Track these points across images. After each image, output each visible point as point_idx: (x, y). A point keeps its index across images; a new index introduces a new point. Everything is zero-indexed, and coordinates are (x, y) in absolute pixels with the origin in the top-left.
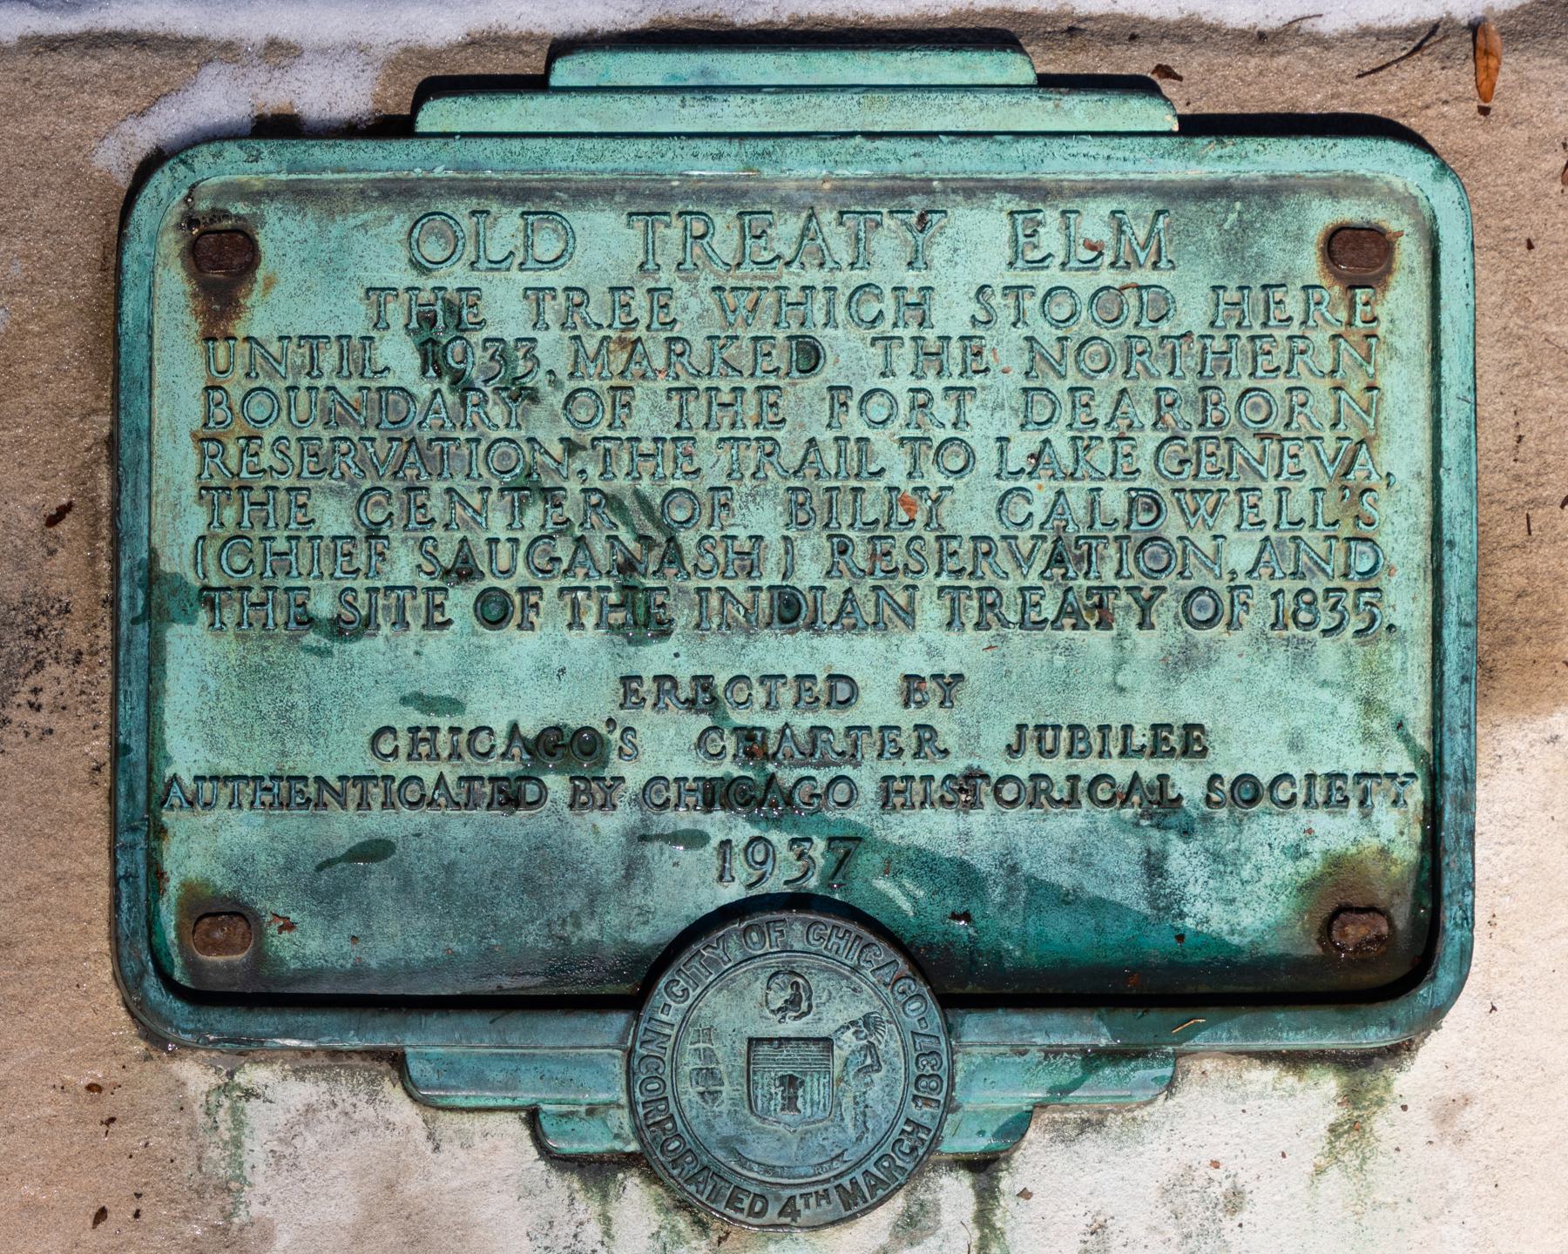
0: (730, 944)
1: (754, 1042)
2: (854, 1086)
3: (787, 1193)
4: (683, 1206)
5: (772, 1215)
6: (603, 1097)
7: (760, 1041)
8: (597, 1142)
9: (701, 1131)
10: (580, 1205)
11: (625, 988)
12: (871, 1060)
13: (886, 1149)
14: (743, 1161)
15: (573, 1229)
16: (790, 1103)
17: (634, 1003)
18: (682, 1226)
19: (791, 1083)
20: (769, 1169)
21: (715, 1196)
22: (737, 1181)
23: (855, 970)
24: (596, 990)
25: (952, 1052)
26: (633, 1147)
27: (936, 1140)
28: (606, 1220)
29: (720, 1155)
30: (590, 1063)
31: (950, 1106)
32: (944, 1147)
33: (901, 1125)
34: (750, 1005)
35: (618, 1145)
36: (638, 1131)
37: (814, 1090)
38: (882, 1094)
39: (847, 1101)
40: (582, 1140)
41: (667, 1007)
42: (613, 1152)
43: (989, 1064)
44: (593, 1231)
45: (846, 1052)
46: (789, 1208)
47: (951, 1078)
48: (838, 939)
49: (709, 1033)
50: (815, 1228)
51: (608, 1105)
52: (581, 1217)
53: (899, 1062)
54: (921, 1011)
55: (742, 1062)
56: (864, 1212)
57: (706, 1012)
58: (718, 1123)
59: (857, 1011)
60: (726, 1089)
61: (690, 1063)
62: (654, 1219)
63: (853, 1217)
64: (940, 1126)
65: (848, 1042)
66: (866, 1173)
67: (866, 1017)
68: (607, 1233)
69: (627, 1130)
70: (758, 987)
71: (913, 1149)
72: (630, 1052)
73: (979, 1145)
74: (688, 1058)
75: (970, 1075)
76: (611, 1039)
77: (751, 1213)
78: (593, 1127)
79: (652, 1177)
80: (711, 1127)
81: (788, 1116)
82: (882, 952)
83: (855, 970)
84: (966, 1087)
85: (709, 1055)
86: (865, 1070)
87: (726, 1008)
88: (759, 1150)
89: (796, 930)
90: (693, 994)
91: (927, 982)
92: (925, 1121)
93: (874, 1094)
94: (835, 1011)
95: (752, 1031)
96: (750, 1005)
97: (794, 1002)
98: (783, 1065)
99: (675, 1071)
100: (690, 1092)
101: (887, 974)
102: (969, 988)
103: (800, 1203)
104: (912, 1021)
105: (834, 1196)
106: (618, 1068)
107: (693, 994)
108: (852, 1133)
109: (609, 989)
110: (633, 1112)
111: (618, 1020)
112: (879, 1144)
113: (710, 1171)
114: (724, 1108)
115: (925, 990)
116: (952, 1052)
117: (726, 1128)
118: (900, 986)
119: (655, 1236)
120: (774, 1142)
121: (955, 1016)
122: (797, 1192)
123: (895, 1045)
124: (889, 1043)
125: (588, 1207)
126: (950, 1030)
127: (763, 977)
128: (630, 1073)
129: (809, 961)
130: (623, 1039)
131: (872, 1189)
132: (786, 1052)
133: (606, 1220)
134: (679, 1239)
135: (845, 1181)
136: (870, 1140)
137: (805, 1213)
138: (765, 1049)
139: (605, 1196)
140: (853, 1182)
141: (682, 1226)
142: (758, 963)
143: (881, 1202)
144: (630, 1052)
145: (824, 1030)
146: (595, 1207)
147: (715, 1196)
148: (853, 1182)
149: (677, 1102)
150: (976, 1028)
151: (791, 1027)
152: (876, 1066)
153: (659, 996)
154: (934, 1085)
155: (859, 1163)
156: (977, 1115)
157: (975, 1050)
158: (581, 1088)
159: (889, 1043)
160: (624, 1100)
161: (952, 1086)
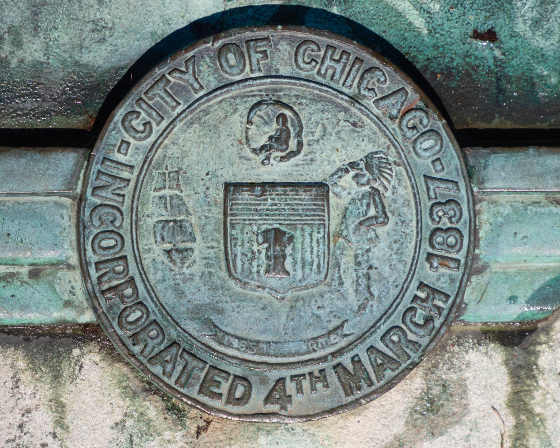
0: (203, 66)
1: (231, 188)
2: (356, 242)
3: (274, 375)
4: (151, 388)
5: (256, 402)
6: (50, 255)
7: (239, 186)
8: (43, 312)
9: (168, 298)
10: (26, 389)
11: (77, 121)
12: (375, 207)
13: (395, 319)
14: (219, 334)
15: (18, 418)
16: (277, 263)
17: (83, 139)
18: (152, 413)
19: (277, 238)
20: (254, 345)
21: (186, 378)
22: (212, 360)
23: (354, 99)
24: (40, 123)
25: (474, 201)
26: (88, 317)
27: (458, 307)
28: (59, 406)
29: (192, 327)
30: (32, 214)
31: (473, 267)
32: (468, 316)
33: (413, 290)
34: (226, 142)
35: (69, 315)
36: (91, 296)
37: (306, 245)
38: (390, 251)
39: (347, 261)
40: (25, 308)
41: (125, 143)
42: (65, 323)
43: (520, 214)
44: (42, 421)
45: (345, 201)
46: (277, 393)
47: (474, 232)
48: (335, 62)
49: (176, 177)
50: (308, 417)
51: (56, 265)
52: (28, 402)
53: (410, 213)
54: (435, 150)
55: (217, 213)
56: (369, 397)
57: (174, 151)
58: (189, 288)
59: (358, 150)
60: (198, 246)
61: (153, 213)
62: (115, 405)
63: (356, 403)
64: (460, 291)
65: (347, 189)
66: (371, 348)
67: (369, 157)
68: (60, 422)
69: (80, 296)
70: (237, 120)
71: (428, 320)
72: (81, 200)
73: (510, 314)
74: (151, 208)
75: (497, 229)
76: (57, 185)
77: (231, 399)
78: (38, 291)
79: (112, 354)
80: (180, 294)
81: (273, 280)
82: (388, 78)
83: (354, 99)
84: (492, 243)
85: (176, 204)
86: (366, 222)
87: (195, 148)
88: (240, 320)
89: (282, 49)
90: (157, 129)
91: (444, 113)
92: (443, 285)
93: (379, 252)
94: (331, 149)
95: (229, 176)
96: (226, 142)
97: (279, 140)
98: (272, 217)
99: (136, 224)
100: (153, 251)
101: (394, 105)
102: (497, 123)
103: (291, 387)
104: (424, 163)
105: (332, 377)
106: (67, 220)
107: (157, 129)
108: (353, 300)
109: (57, 122)
110: (85, 275)
111: (66, 160)
112: (386, 314)
113: (181, 348)
114: (197, 269)
115: (440, 124)
116: (474, 201)
117: (199, 295)
118: (410, 119)
119: (119, 425)
120: (258, 312)
121: (478, 156)
122: (286, 373)
123: (405, 192)
124: (398, 190)
125: (35, 390)
126: (470, 174)
127: (243, 108)
128: (81, 226)
129: (298, 88)
130: (71, 184)
131: (379, 368)
132: (272, 200)
133: (59, 406)
134: (149, 430)
135: (346, 360)
136: (376, 309)
137: (297, 398)
138: (245, 196)
139: (57, 377)
140: (356, 360)
141: (152, 413)
142: (235, 91)
143: (390, 385)
144: (81, 200)
145: (316, 174)
146: (45, 391)
147: (186, 378)
148: (356, 360)
149: (139, 262)
150: (503, 170)
151: (277, 170)
152: (383, 217)
153: (114, 132)
154: (452, 239)
155: (362, 337)
156: (507, 277)
157: (503, 198)
158: (21, 245)
159: (398, 190)
160: (74, 260)
161: (475, 241)
